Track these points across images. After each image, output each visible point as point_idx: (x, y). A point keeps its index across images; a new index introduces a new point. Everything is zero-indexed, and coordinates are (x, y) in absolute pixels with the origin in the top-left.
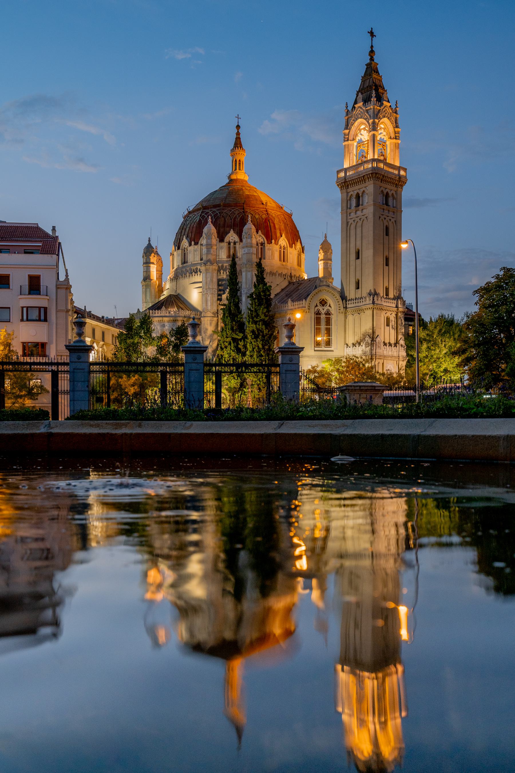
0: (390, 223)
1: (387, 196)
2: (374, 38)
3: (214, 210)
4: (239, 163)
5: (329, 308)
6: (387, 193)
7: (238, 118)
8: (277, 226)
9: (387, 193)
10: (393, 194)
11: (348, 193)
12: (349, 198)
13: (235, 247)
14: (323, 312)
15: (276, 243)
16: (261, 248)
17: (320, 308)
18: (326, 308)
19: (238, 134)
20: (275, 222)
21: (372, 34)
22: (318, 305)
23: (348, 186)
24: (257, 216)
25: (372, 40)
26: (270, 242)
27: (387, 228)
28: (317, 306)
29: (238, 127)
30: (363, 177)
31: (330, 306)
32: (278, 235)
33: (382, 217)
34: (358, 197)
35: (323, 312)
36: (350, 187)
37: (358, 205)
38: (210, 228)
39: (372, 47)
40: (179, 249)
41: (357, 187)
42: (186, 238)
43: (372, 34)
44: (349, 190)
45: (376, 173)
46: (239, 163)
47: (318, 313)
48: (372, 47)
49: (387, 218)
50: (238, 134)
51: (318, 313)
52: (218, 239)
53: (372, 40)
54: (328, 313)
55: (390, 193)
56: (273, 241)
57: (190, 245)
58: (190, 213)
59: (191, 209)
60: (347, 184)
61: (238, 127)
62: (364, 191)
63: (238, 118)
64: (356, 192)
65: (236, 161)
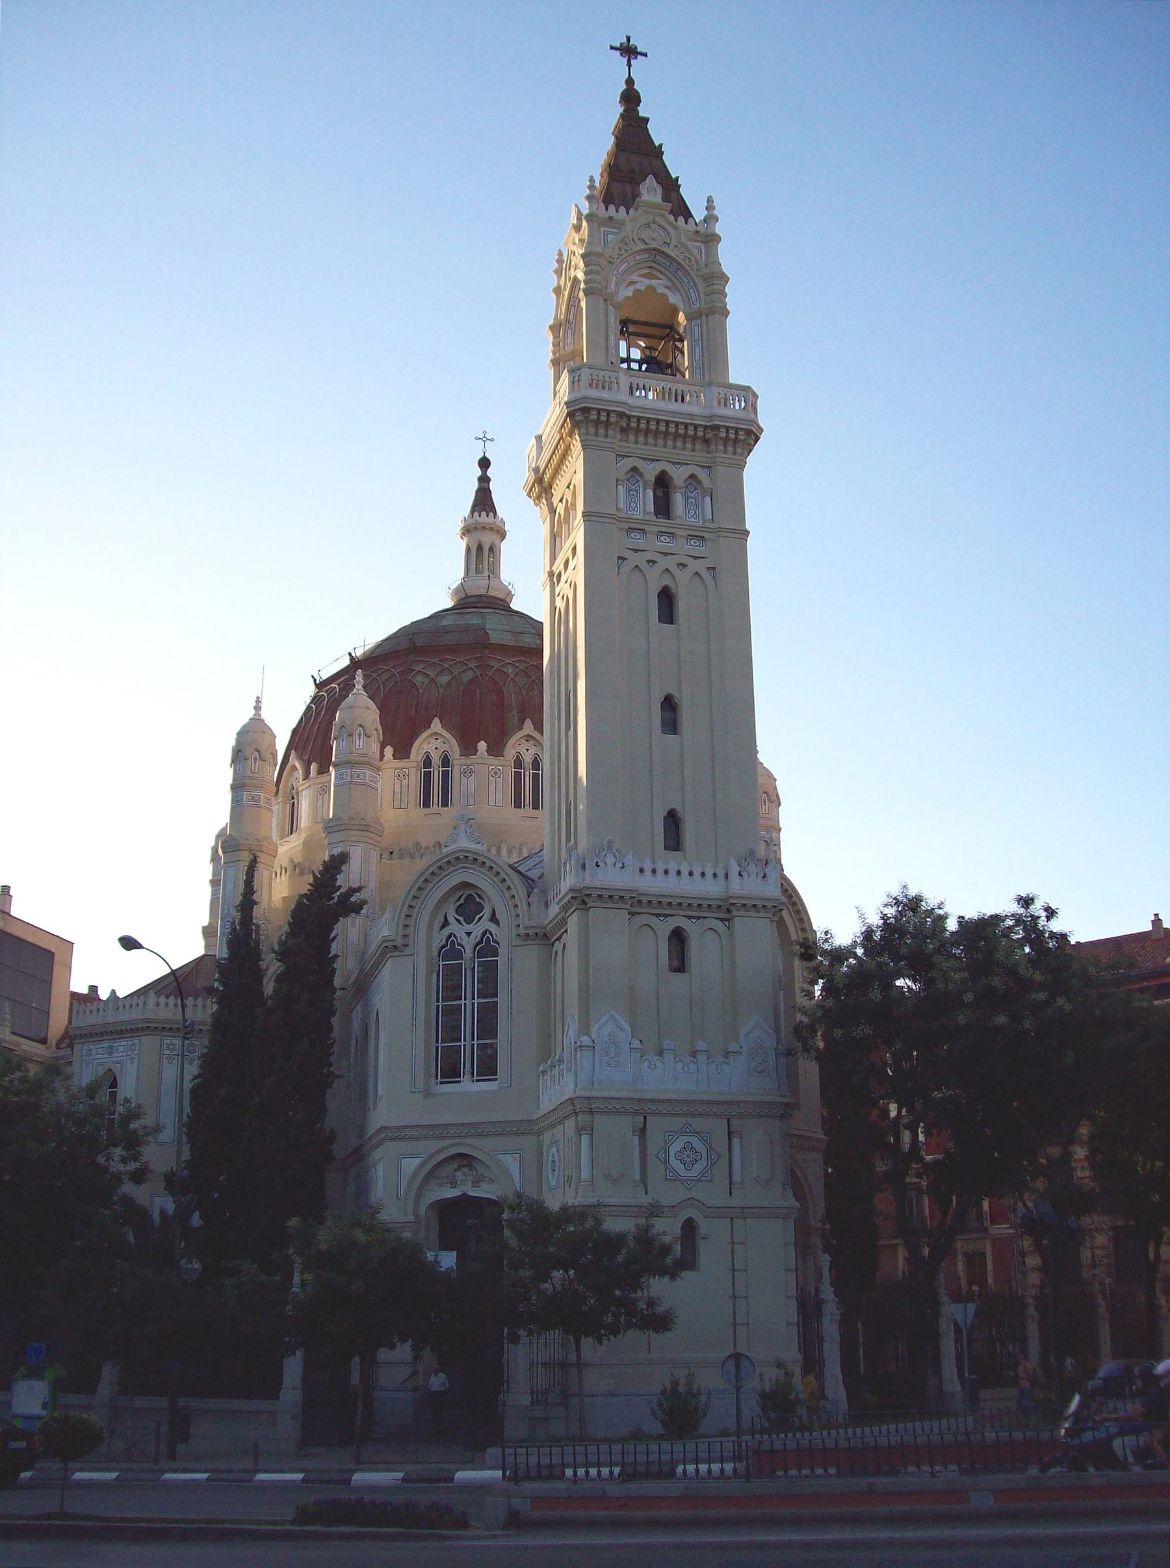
0: (683, 577)
1: (663, 482)
2: (637, 63)
5: (492, 927)
11: (553, 511)
14: (468, 944)
15: (496, 749)
16: (445, 775)
17: (457, 929)
18: (477, 929)
19: (484, 480)
21: (629, 51)
22: (451, 919)
25: (629, 65)
26: (468, 749)
27: (667, 599)
28: (446, 923)
29: (484, 463)
31: (494, 919)
35: (468, 944)
39: (630, 82)
43: (629, 51)
45: (585, 410)
47: (451, 950)
48: (630, 82)
49: (670, 563)
50: (484, 480)
51: (451, 950)
53: (629, 65)
54: (487, 947)
55: (678, 475)
56: (482, 746)
61: (484, 463)
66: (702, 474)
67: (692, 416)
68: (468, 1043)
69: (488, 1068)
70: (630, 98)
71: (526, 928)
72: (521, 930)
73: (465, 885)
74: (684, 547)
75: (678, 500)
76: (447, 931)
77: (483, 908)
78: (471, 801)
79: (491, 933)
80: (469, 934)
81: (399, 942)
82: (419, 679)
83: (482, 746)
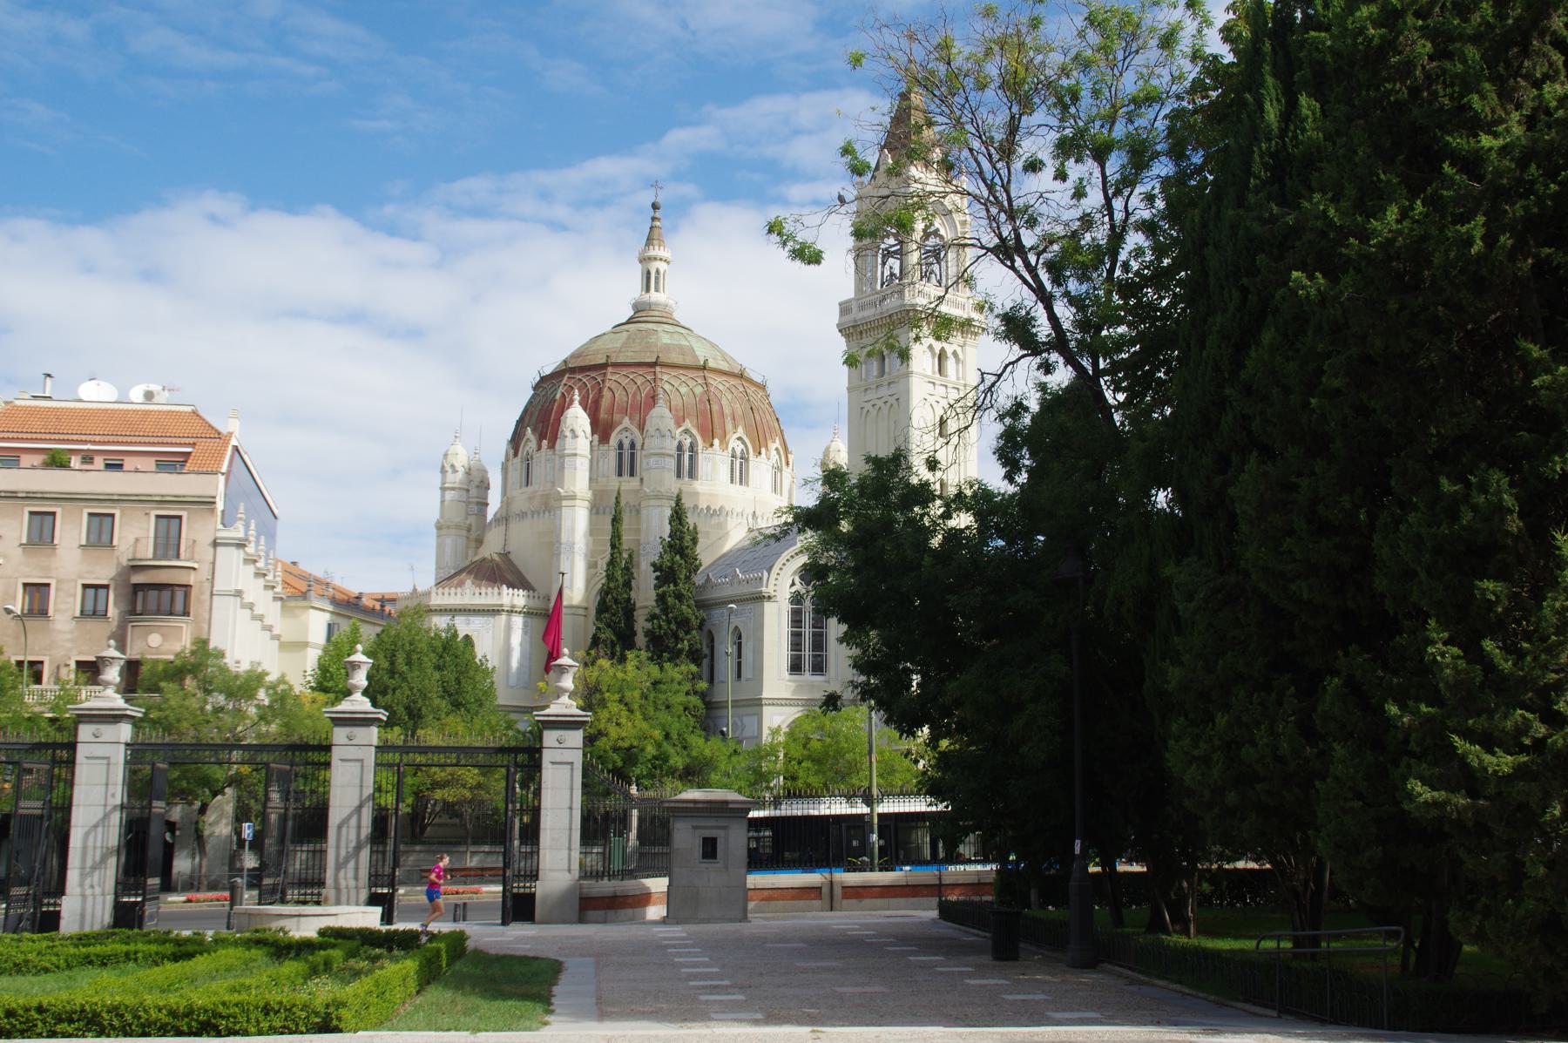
3: (593, 374)
6: (943, 351)
8: (727, 411)
9: (943, 351)
10: (955, 353)
13: (632, 455)
20: (724, 402)
24: (683, 390)
32: (729, 426)
33: (932, 400)
37: (882, 373)
38: (577, 418)
40: (516, 454)
42: (534, 431)
52: (596, 437)
56: (716, 442)
57: (539, 448)
58: (543, 379)
59: (548, 371)
65: (649, 273)
66: (959, 350)
68: (807, 653)
69: (819, 667)
75: (950, 364)
82: (667, 387)
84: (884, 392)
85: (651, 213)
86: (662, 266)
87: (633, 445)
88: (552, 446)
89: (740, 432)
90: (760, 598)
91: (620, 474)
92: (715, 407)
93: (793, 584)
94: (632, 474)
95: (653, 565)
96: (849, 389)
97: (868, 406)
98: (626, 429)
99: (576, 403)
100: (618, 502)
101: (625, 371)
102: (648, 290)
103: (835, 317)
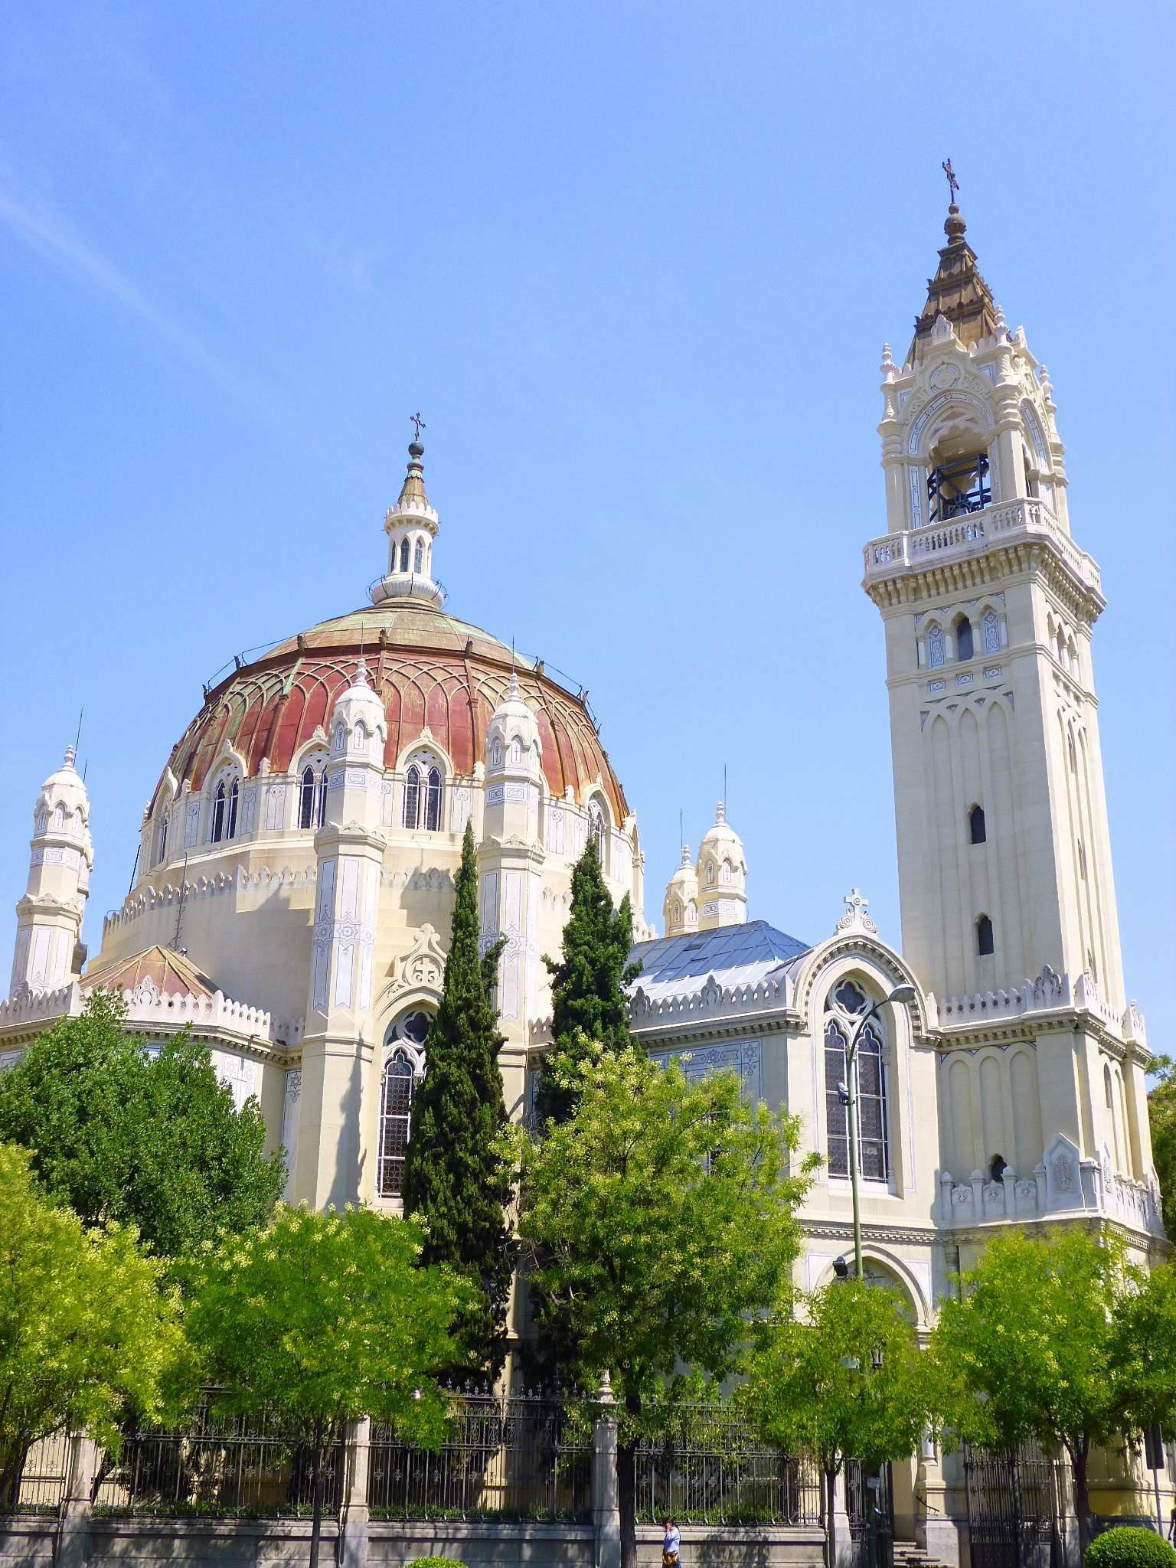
4: (418, 553)
7: (416, 419)
8: (576, 748)
12: (920, 632)
14: (851, 1033)
23: (916, 590)
30: (987, 558)
34: (963, 626)
35: (851, 1033)
36: (925, 594)
37: (965, 650)
40: (197, 786)
41: (955, 596)
44: (920, 606)
46: (418, 553)
55: (1067, 631)
56: (570, 789)
60: (912, 584)
61: (415, 450)
62: (987, 607)
63: (416, 419)
64: (952, 613)
65: (406, 543)
67: (1081, 582)
70: (954, 228)
71: (929, 1032)
72: (923, 1033)
73: (856, 973)
74: (1072, 701)
76: (830, 1014)
77: (863, 1000)
78: (560, 850)
79: (871, 1027)
80: (852, 1024)
81: (804, 1018)
83: (570, 789)
84: (980, 682)
85: (408, 459)
86: (427, 538)
87: (434, 778)
88: (281, 768)
89: (599, 780)
90: (787, 1026)
91: (410, 822)
92: (562, 738)
93: (827, 1008)
94: (434, 824)
95: (546, 960)
96: (891, 684)
97: (935, 710)
98: (425, 749)
99: (362, 678)
100: (468, 841)
101: (412, 659)
102: (404, 567)
103: (858, 572)
